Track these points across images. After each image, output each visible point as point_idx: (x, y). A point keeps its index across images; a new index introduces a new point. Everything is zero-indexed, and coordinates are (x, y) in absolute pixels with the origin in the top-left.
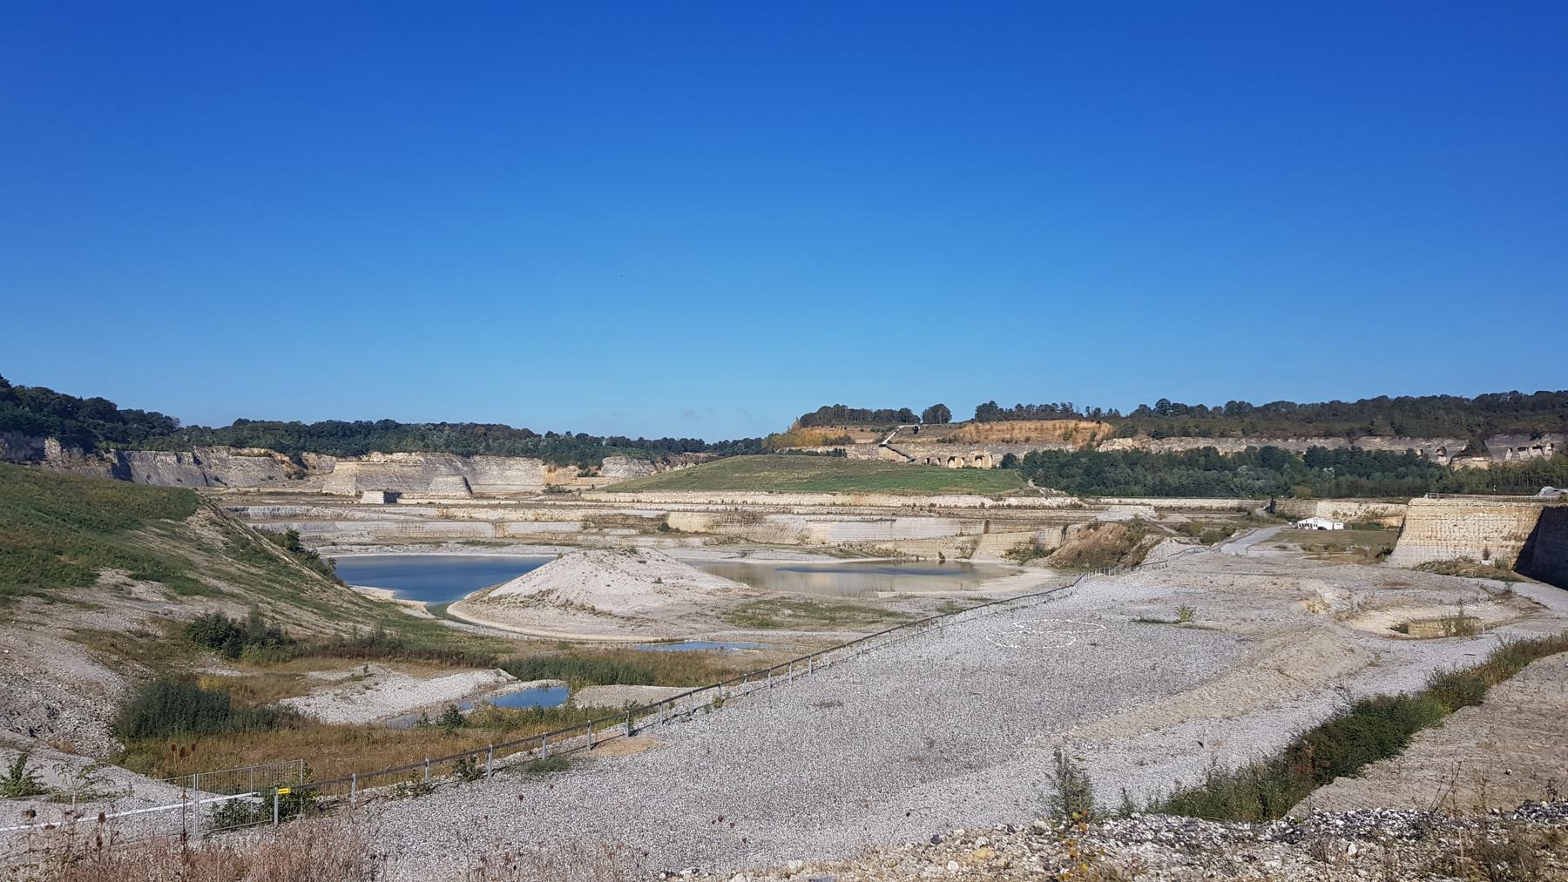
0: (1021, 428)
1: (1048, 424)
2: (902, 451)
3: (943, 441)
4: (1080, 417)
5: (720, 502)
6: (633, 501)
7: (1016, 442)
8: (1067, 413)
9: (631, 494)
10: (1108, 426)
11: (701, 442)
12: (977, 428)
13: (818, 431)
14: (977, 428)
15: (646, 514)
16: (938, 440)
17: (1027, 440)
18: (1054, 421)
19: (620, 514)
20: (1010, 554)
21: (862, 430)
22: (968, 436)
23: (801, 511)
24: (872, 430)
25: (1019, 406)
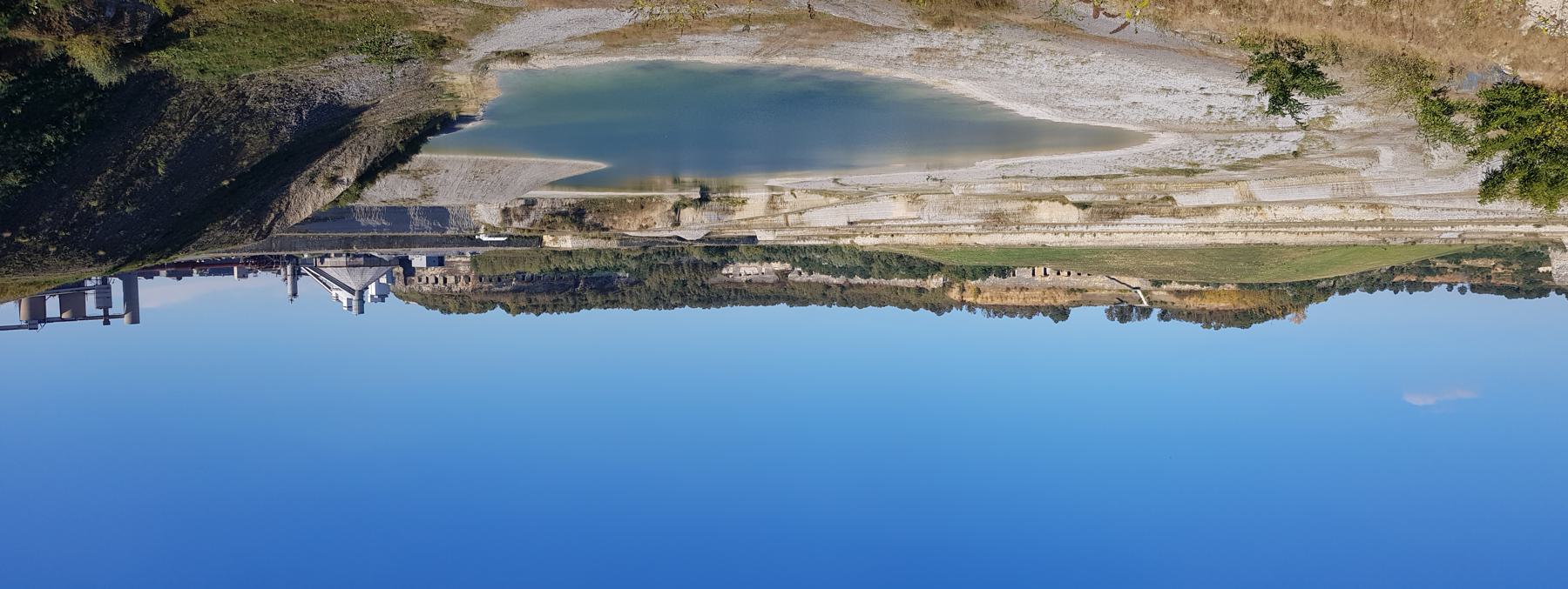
1: (997, 302)
2: (1116, 283)
4: (982, 307)
5: (1099, 235)
6: (1214, 233)
7: (1016, 288)
8: (1000, 311)
9: (1222, 242)
10: (952, 297)
11: (1509, 296)
13: (1223, 305)
14: (1055, 301)
15: (1146, 219)
16: (1087, 291)
17: (1008, 289)
18: (994, 303)
19: (1184, 218)
20: (743, 202)
21: (1173, 303)
22: (1062, 295)
23: (967, 227)
24: (1166, 303)
25: (1030, 317)
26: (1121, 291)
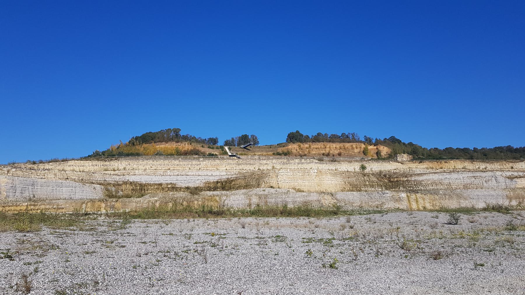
0: (330, 147)
1: (348, 145)
3: (279, 154)
12: (300, 146)
18: (351, 144)
22: (294, 151)
26: (245, 154)
